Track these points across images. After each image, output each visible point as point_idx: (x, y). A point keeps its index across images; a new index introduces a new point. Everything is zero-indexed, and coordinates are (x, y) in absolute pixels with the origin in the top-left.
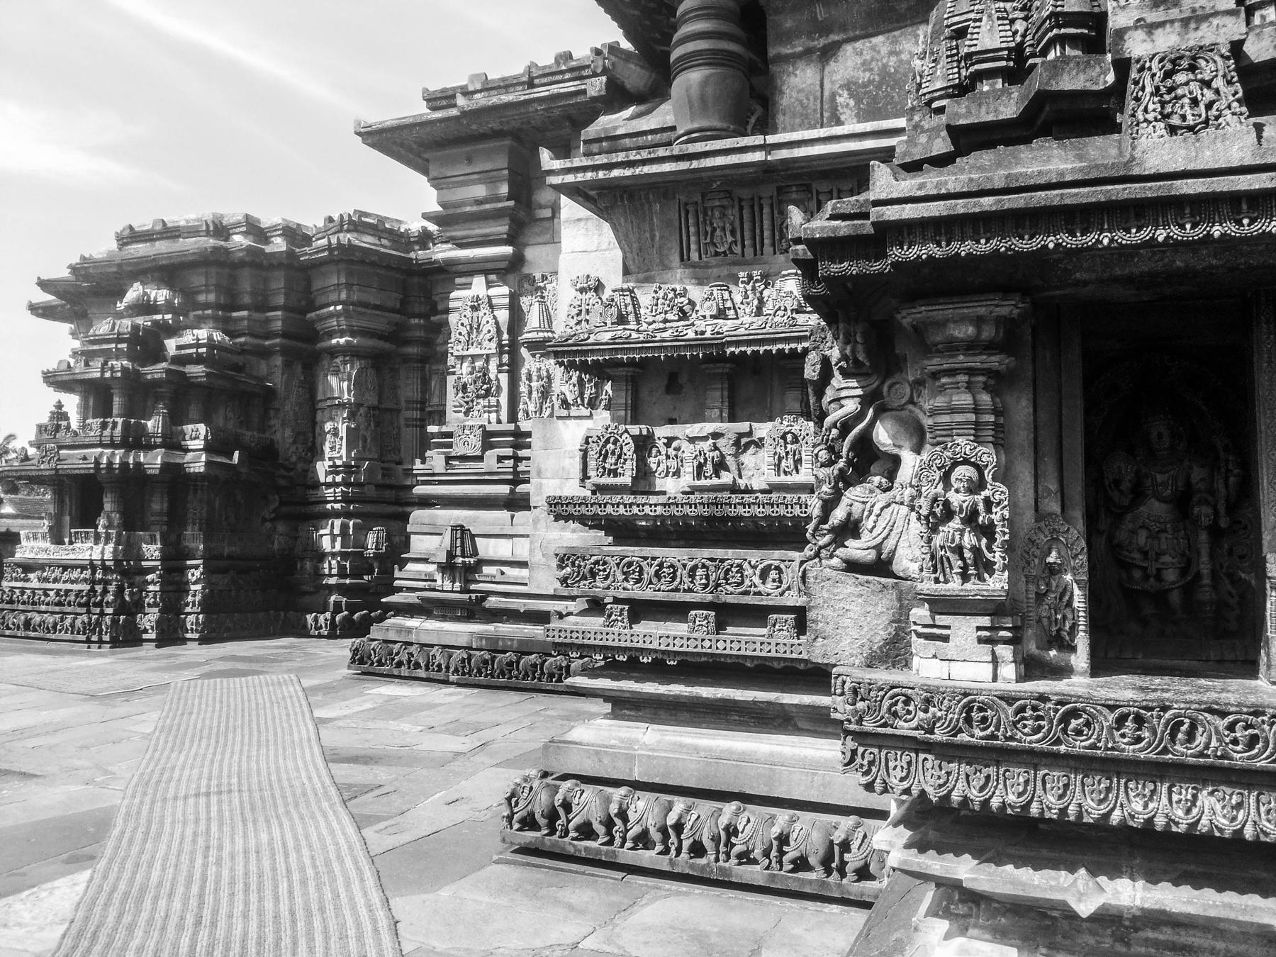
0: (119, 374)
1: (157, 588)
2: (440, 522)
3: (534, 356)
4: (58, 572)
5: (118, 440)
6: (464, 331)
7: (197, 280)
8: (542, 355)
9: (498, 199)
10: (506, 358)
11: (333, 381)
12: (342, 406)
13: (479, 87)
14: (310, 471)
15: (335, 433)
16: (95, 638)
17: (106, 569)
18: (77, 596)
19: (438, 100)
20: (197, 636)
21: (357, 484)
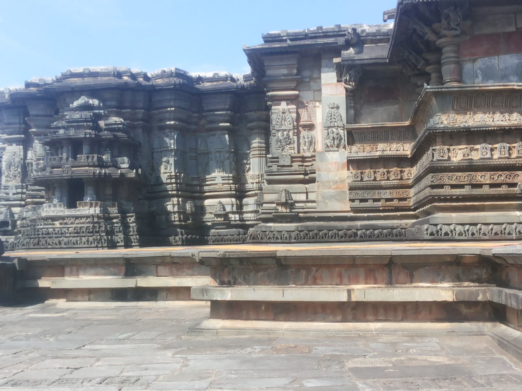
0: (93, 136)
1: (120, 225)
3: (305, 130)
4: (72, 220)
5: (97, 163)
6: (279, 121)
7: (107, 95)
8: (308, 130)
9: (292, 75)
10: (296, 131)
11: (167, 140)
12: (172, 150)
13: (285, 35)
14: (159, 178)
15: (168, 162)
16: (100, 245)
17: (99, 217)
18: (86, 229)
19: (269, 39)
20: (138, 244)
21: (180, 184)
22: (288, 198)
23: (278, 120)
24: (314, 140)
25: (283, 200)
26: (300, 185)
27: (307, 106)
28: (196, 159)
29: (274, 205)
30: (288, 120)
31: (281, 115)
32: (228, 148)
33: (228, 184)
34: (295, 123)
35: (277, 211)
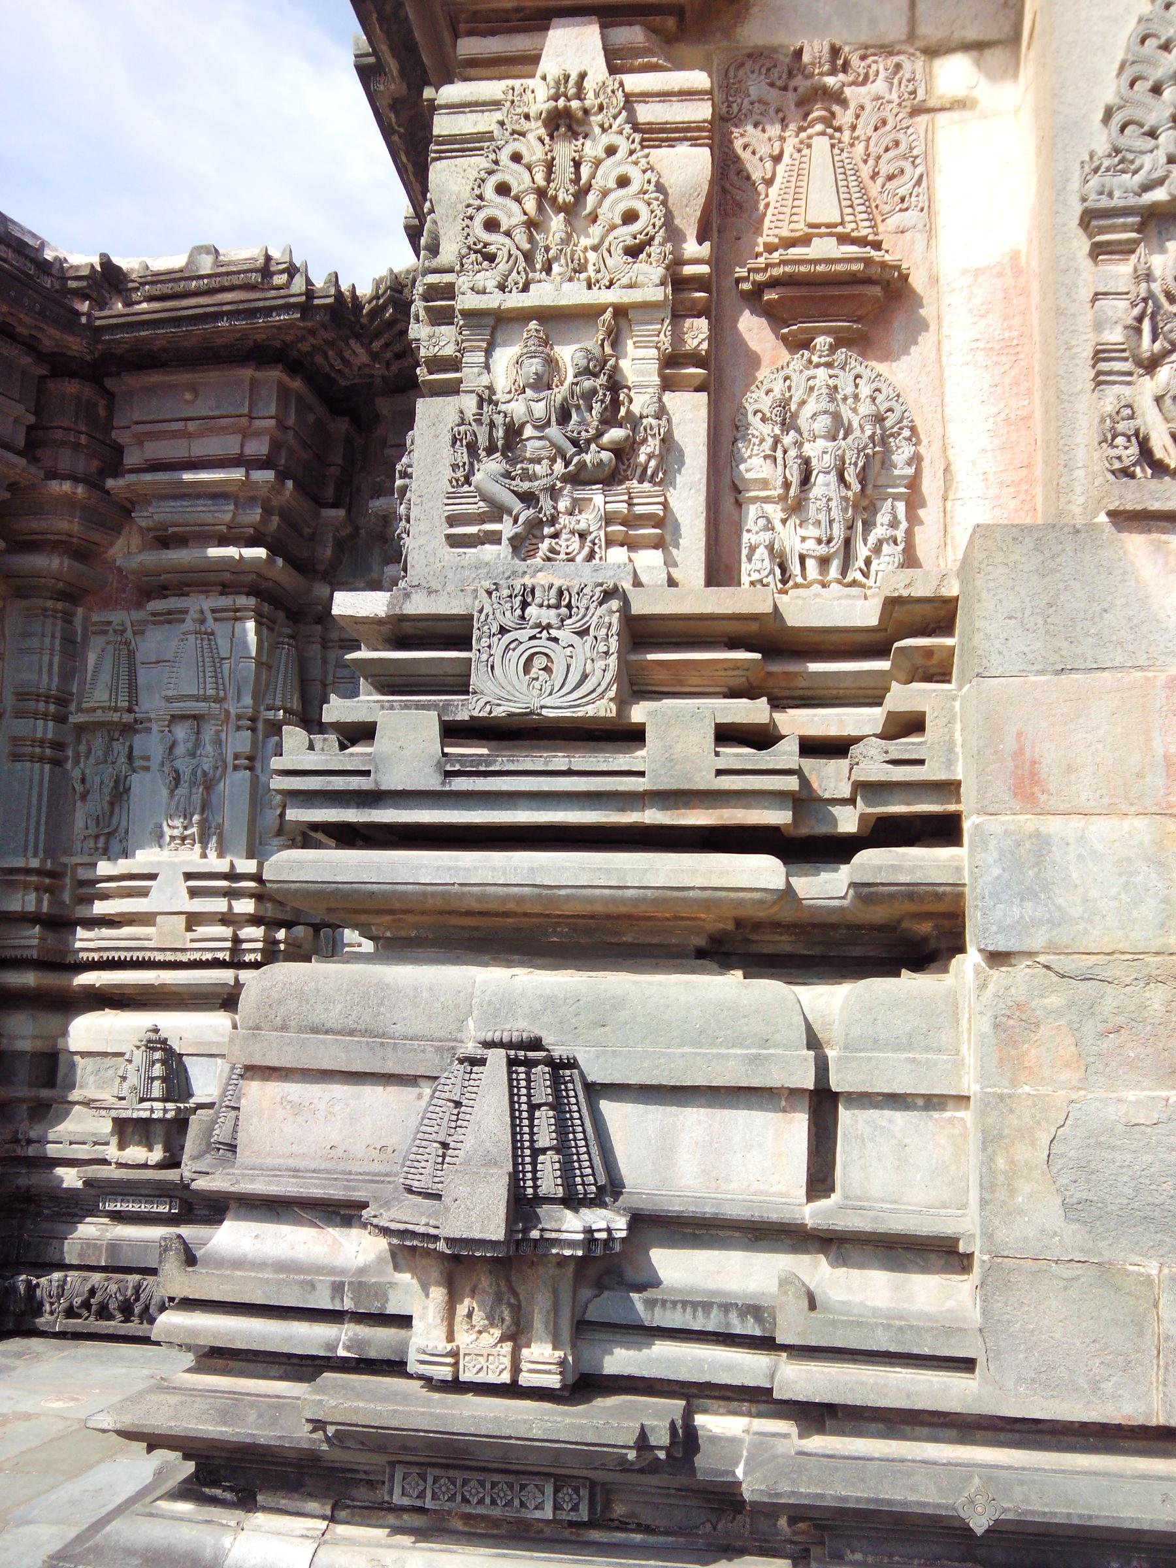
2: (407, 1020)
6: (510, 214)
8: (842, 341)
10: (697, 333)
22: (549, 1181)
23: (499, 207)
24: (902, 454)
25: (479, 1214)
26: (728, 987)
27: (837, 97)
28: (57, 763)
29: (356, 1249)
30: (611, 210)
31: (533, 150)
32: (248, 700)
33: (225, 919)
34: (692, 248)
35: (380, 1339)
